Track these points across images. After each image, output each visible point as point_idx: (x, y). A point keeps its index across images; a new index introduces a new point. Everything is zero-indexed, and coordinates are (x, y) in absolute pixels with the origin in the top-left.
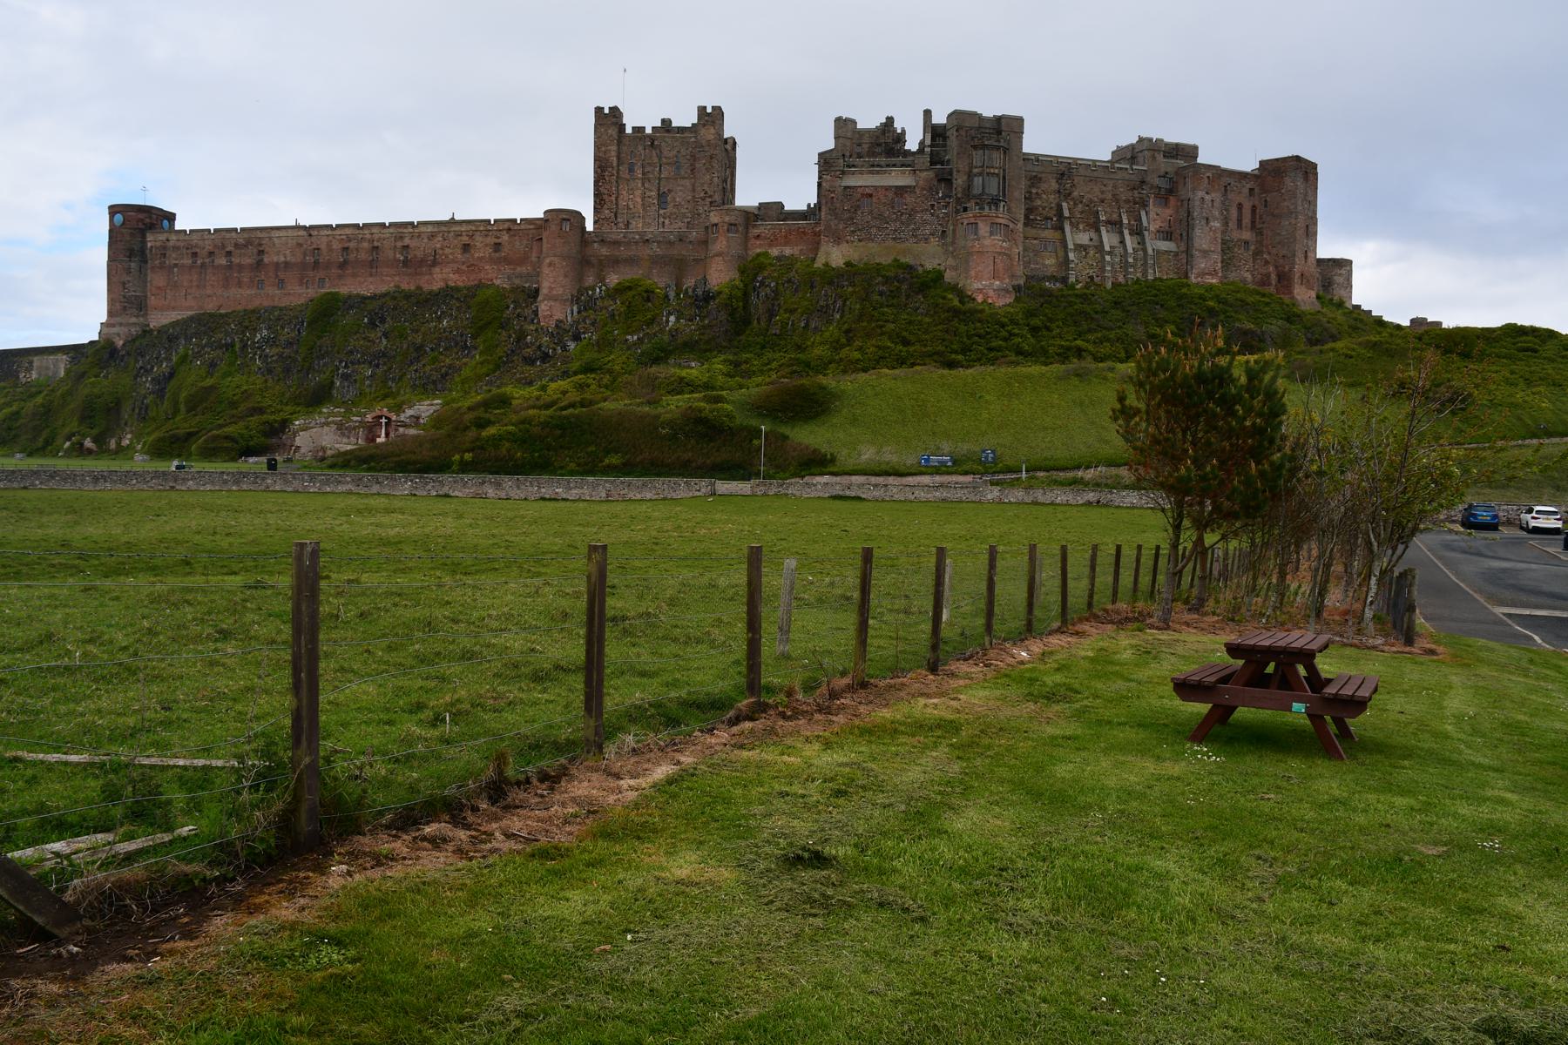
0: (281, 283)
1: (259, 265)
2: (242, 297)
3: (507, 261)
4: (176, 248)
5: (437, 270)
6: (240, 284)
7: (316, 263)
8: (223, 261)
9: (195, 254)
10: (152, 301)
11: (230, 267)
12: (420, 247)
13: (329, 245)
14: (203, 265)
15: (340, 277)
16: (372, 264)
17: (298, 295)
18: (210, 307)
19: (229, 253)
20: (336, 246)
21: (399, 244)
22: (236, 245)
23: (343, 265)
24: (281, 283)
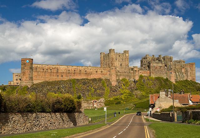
0: (62, 76)
1: (58, 72)
2: (54, 78)
3: (103, 74)
4: (39, 68)
5: (92, 75)
6: (53, 76)
7: (69, 73)
8: (50, 71)
9: (43, 69)
10: (34, 78)
11: (51, 72)
12: (88, 71)
13: (71, 69)
14: (45, 72)
15: (74, 75)
16: (80, 73)
17: (65, 78)
18: (47, 80)
19: (51, 70)
20: (73, 70)
21: (85, 70)
22: (53, 68)
23: (74, 73)
24: (62, 76)
